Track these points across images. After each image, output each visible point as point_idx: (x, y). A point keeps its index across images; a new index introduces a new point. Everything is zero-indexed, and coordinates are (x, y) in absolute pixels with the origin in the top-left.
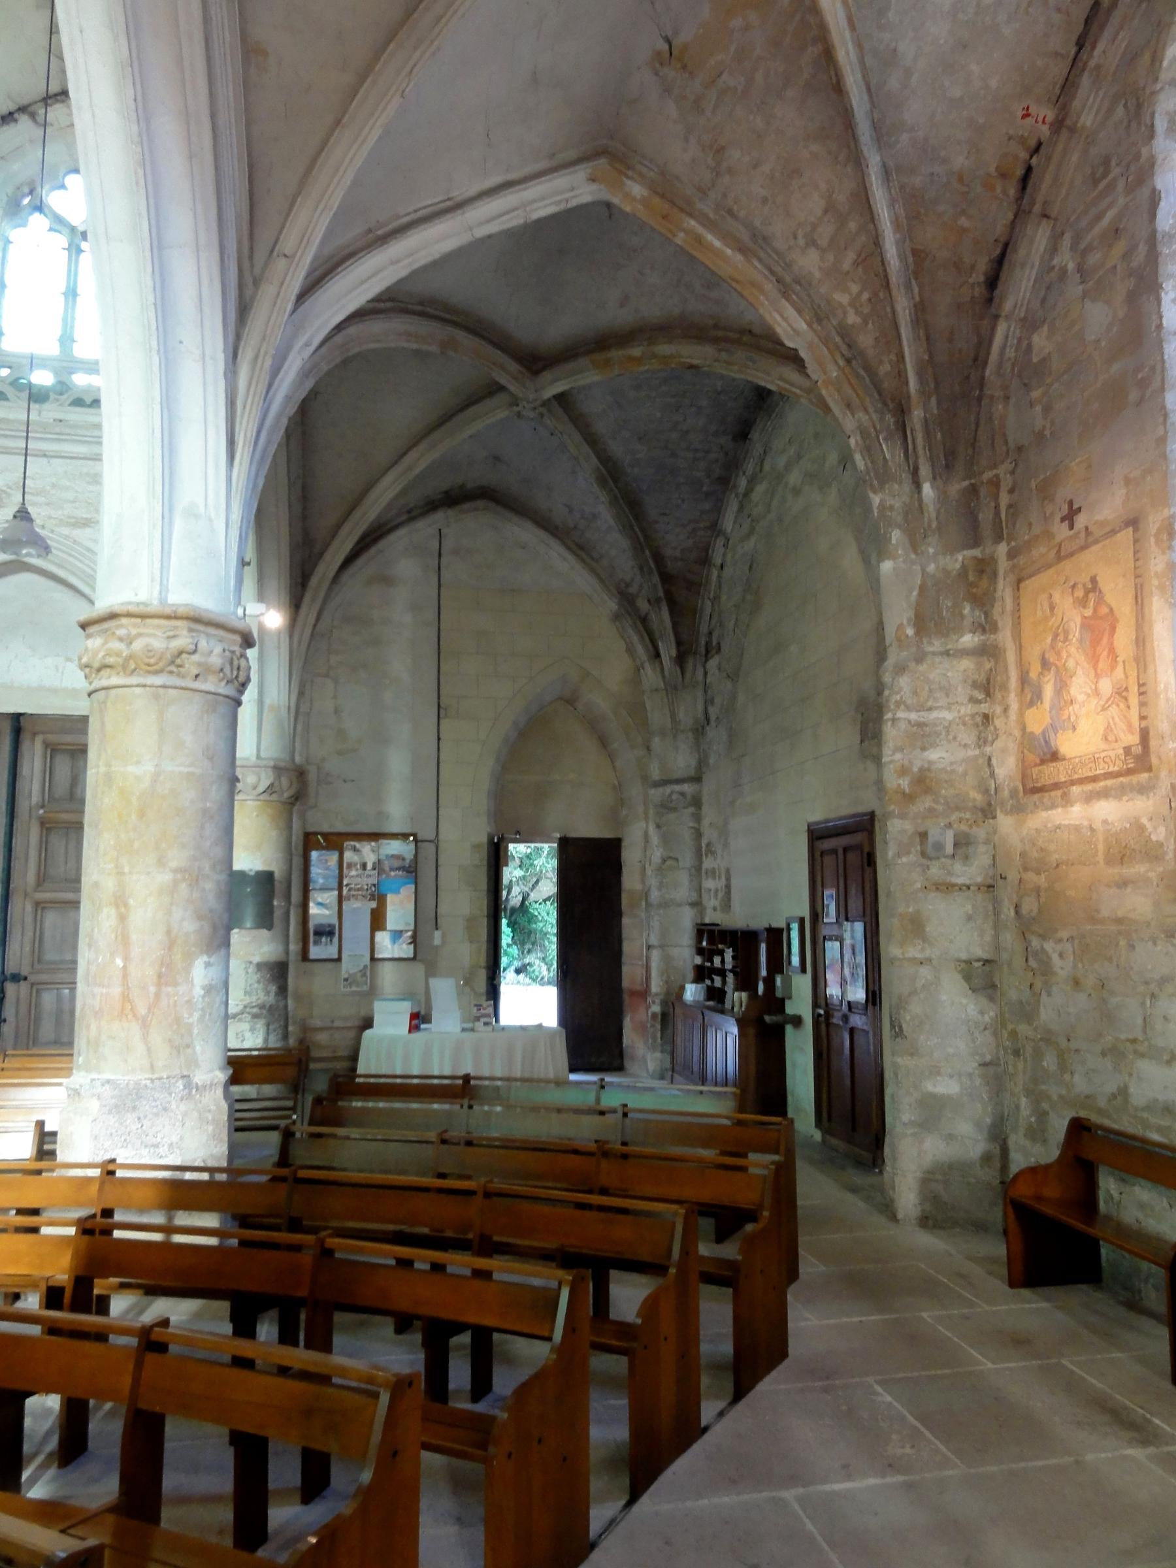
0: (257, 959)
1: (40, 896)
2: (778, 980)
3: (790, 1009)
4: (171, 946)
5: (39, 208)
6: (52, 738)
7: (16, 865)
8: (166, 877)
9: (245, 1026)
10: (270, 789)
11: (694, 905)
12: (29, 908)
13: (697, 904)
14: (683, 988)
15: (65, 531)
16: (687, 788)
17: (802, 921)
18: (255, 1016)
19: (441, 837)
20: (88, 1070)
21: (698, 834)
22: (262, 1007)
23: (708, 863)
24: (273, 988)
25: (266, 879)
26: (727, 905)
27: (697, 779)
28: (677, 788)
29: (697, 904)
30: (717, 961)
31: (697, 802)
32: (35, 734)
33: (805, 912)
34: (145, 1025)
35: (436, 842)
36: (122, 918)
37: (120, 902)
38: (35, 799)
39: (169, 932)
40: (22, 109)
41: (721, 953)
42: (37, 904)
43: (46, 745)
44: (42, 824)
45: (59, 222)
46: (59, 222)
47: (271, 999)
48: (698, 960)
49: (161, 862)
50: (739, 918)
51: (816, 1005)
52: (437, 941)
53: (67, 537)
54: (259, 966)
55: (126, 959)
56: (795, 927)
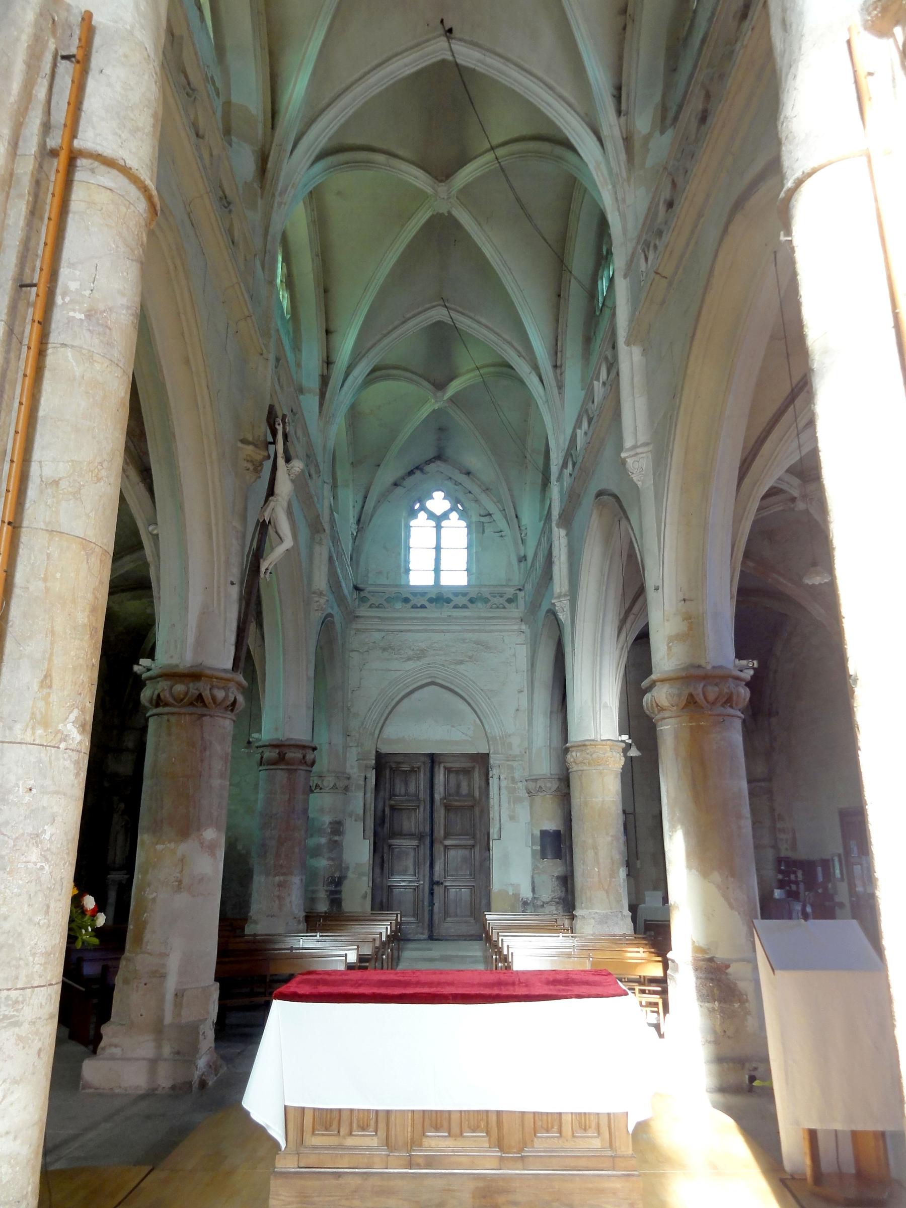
0: (556, 874)
1: (448, 842)
2: (830, 886)
3: (837, 899)
4: (613, 863)
5: (423, 508)
6: (448, 765)
7: (436, 827)
8: (609, 839)
9: (553, 908)
10: (558, 790)
11: (773, 847)
12: (442, 849)
13: (775, 847)
14: (772, 892)
15: (453, 667)
16: (763, 784)
17: (839, 856)
18: (557, 903)
19: (637, 811)
20: (587, 909)
21: (772, 810)
22: (559, 898)
23: (779, 825)
24: (564, 889)
25: (557, 833)
26: (794, 846)
27: (769, 779)
28: (759, 784)
29: (775, 847)
30: (792, 877)
31: (770, 792)
32: (440, 763)
33: (841, 851)
34: (607, 893)
35: (634, 814)
36: (596, 854)
37: (595, 848)
38: (442, 794)
39: (612, 859)
40: (417, 468)
41: (795, 872)
42: (446, 846)
43: (445, 768)
44: (446, 807)
45: (431, 515)
46: (431, 515)
47: (563, 895)
48: (780, 877)
49: (607, 834)
50: (802, 854)
51: (851, 896)
52: (639, 866)
53: (454, 670)
54: (558, 878)
55: (599, 868)
56: (836, 859)
